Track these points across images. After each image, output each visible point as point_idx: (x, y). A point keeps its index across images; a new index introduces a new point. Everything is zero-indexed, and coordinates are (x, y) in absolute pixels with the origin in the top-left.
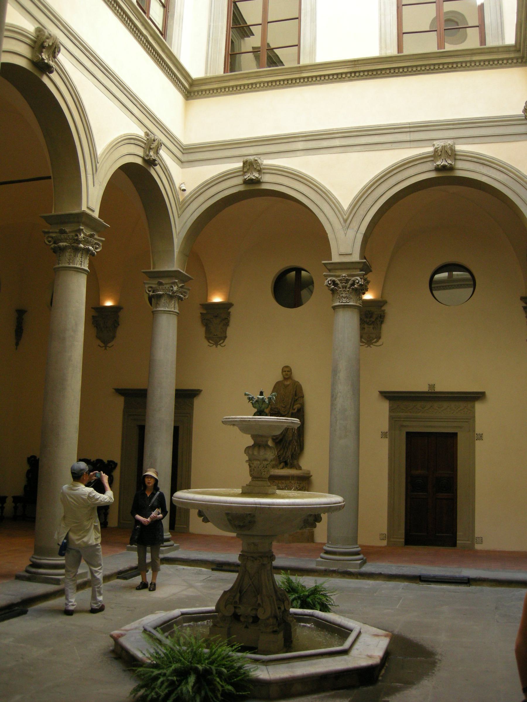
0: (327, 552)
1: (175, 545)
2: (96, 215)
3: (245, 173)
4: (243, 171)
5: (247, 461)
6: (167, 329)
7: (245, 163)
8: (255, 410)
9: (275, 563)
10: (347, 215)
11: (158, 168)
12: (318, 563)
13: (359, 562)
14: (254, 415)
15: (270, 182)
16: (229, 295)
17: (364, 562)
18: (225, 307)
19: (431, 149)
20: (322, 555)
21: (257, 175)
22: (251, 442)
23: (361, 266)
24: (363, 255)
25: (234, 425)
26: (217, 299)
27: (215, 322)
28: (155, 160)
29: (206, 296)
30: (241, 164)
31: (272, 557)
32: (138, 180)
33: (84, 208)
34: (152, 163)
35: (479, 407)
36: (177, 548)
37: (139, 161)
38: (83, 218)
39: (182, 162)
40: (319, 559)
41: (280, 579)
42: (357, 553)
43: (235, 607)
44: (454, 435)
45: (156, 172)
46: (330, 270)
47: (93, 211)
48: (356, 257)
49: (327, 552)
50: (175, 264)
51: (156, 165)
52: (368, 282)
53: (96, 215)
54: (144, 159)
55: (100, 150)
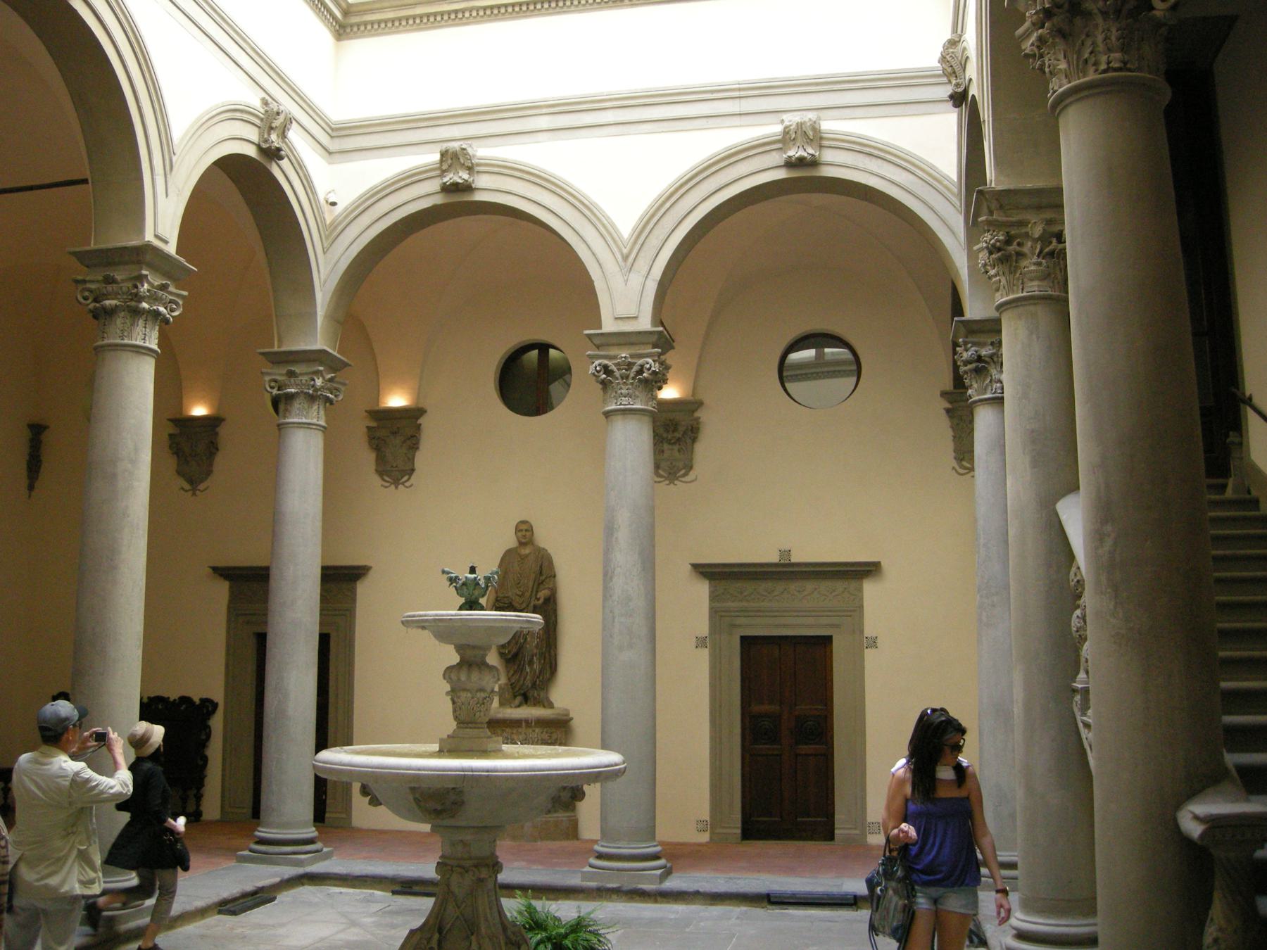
0: (600, 856)
2: (171, 249)
4: (440, 168)
5: (447, 693)
6: (305, 455)
7: (444, 154)
8: (462, 600)
9: (503, 877)
11: (285, 163)
12: (585, 876)
13: (659, 872)
14: (460, 609)
15: (489, 188)
16: (419, 394)
17: (668, 872)
18: (411, 416)
20: (593, 861)
21: (466, 176)
22: (455, 659)
23: (655, 338)
24: (658, 319)
25: (423, 628)
26: (397, 400)
27: (395, 441)
28: (279, 150)
29: (377, 395)
30: (437, 157)
31: (496, 867)
32: (248, 188)
33: (149, 237)
34: (274, 154)
35: (870, 589)
36: (328, 856)
37: (251, 151)
38: (145, 255)
39: (330, 153)
40: (588, 869)
41: (512, 907)
42: (656, 857)
44: (828, 640)
45: (281, 172)
46: (598, 347)
47: (166, 242)
48: (645, 323)
49: (600, 856)
50: (318, 338)
51: (281, 158)
52: (668, 368)
53: (171, 249)
54: (259, 146)
55: (178, 129)
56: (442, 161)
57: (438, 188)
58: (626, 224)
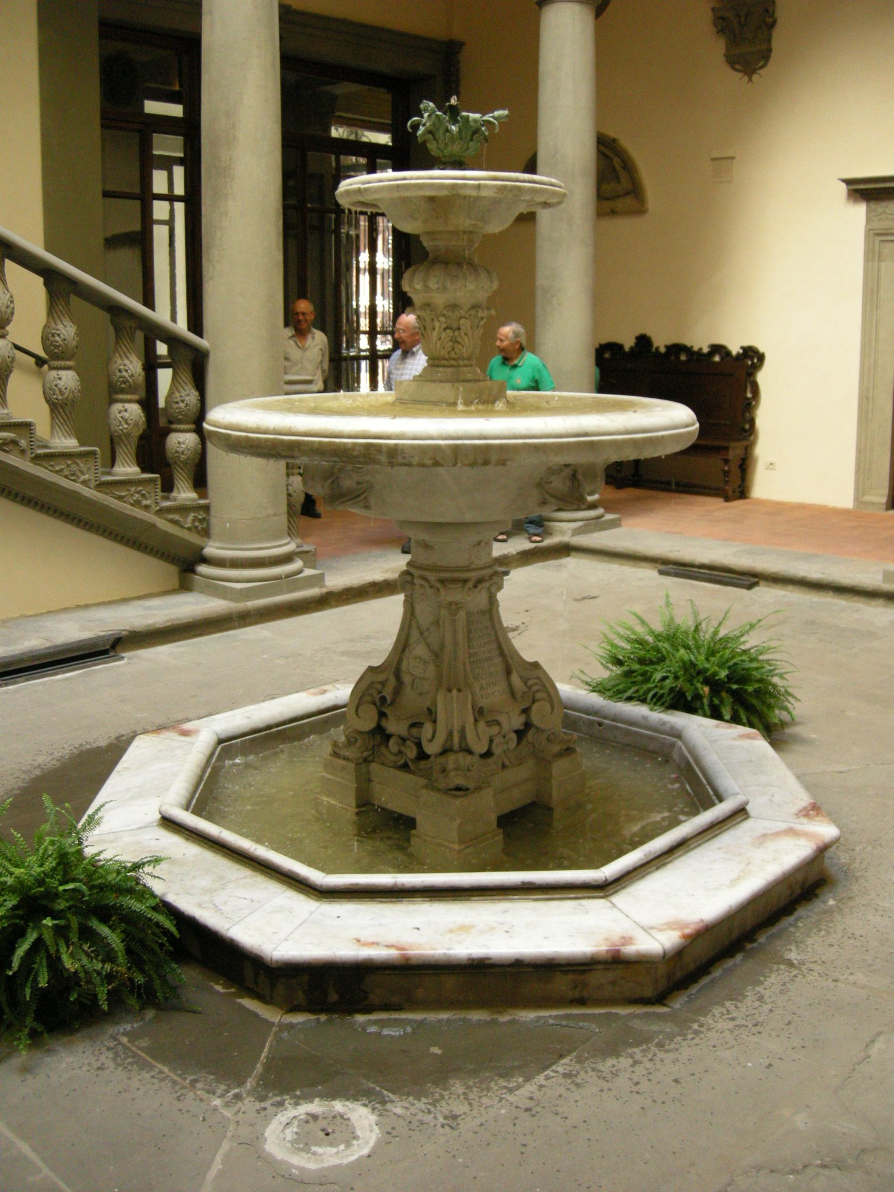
1: (609, 517)
36: (614, 524)
43: (382, 715)
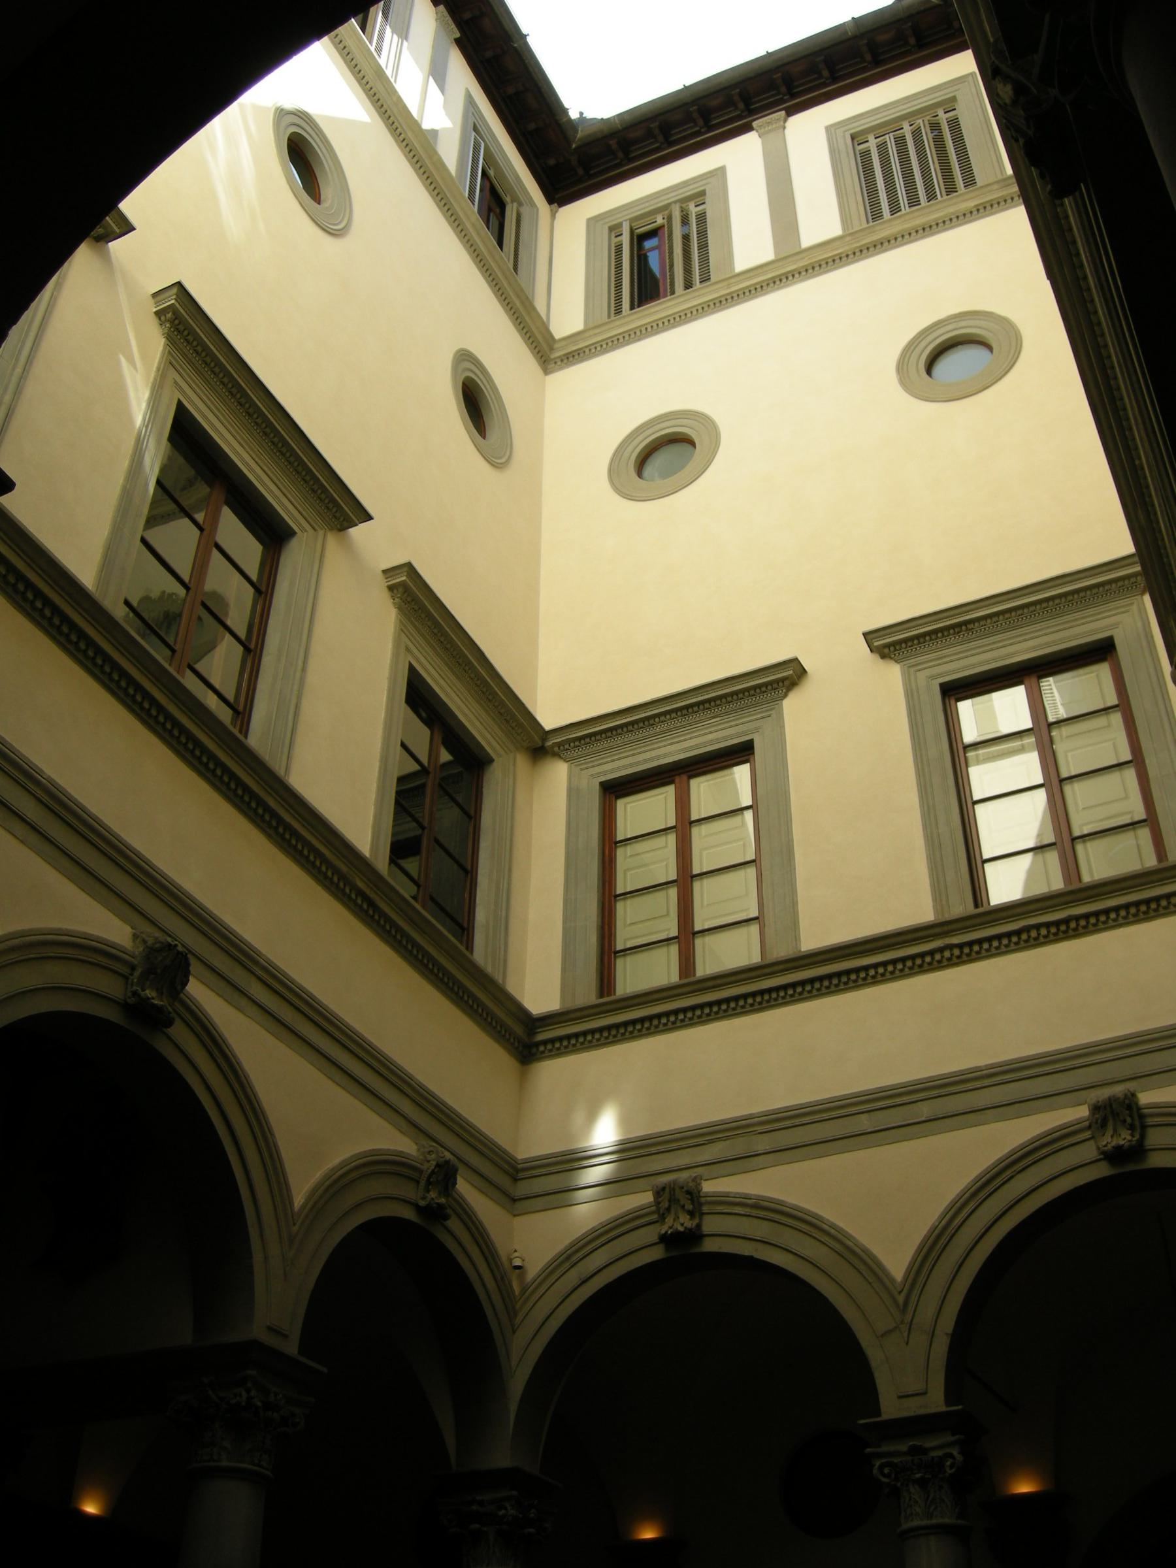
2: (291, 1348)
3: (662, 1218)
4: (657, 1211)
7: (659, 1192)
10: (903, 1294)
15: (723, 1236)
19: (1083, 1112)
24: (952, 1392)
28: (441, 1207)
30: (647, 1198)
33: (258, 1331)
34: (435, 1214)
37: (408, 1214)
47: (285, 1336)
53: (291, 1348)
54: (419, 1209)
56: (657, 1203)
57: (655, 1239)
58: (897, 1264)
